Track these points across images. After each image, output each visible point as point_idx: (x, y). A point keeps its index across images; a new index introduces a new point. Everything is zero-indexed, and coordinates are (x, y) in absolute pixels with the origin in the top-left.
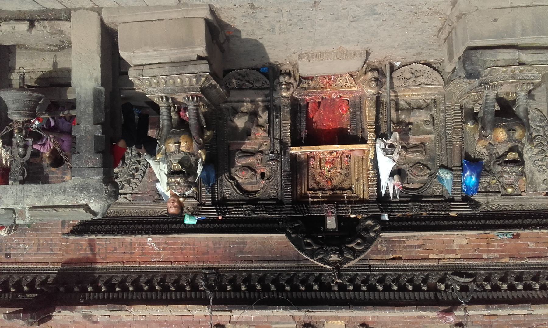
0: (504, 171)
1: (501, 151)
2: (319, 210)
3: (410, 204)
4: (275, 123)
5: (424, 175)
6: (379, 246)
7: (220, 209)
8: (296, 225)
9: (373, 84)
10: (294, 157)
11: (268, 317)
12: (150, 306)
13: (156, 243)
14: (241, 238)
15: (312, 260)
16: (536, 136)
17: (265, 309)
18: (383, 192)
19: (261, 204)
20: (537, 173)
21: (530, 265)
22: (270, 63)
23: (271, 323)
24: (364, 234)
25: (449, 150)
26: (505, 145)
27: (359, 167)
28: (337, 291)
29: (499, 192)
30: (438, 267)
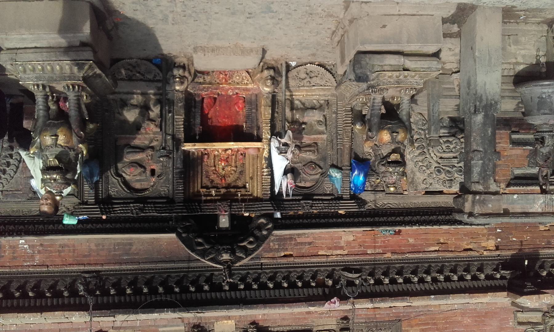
0: (387, 171)
1: (385, 151)
2: (212, 209)
4: (168, 117)
5: (316, 174)
6: (271, 244)
7: (105, 208)
9: (269, 82)
10: (187, 154)
11: (155, 320)
12: (22, 314)
13: (29, 245)
14: (127, 239)
15: (203, 260)
16: (418, 139)
17: (152, 312)
18: (277, 190)
19: (150, 203)
20: (418, 174)
21: (409, 260)
22: (163, 55)
23: (158, 326)
24: (257, 233)
25: (339, 150)
26: (389, 146)
27: (253, 165)
28: (228, 291)
29: (384, 191)
30: (327, 263)
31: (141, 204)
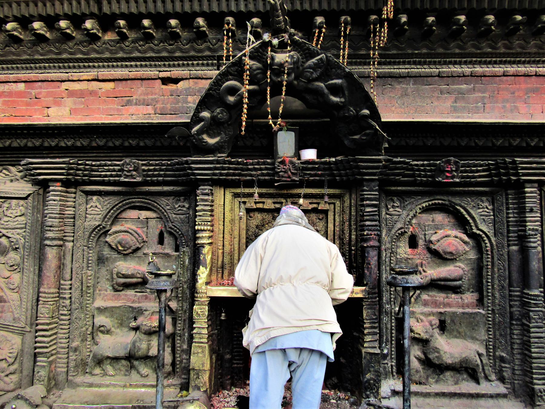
3: (139, 179)
8: (357, 137)
19: (422, 184)
30: (99, 67)
31: (440, 182)
